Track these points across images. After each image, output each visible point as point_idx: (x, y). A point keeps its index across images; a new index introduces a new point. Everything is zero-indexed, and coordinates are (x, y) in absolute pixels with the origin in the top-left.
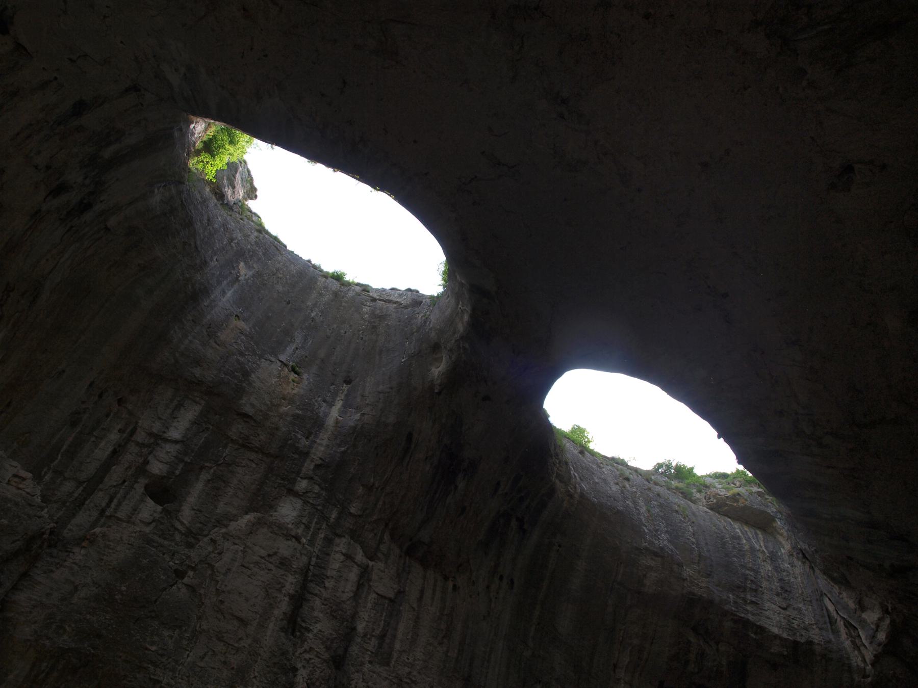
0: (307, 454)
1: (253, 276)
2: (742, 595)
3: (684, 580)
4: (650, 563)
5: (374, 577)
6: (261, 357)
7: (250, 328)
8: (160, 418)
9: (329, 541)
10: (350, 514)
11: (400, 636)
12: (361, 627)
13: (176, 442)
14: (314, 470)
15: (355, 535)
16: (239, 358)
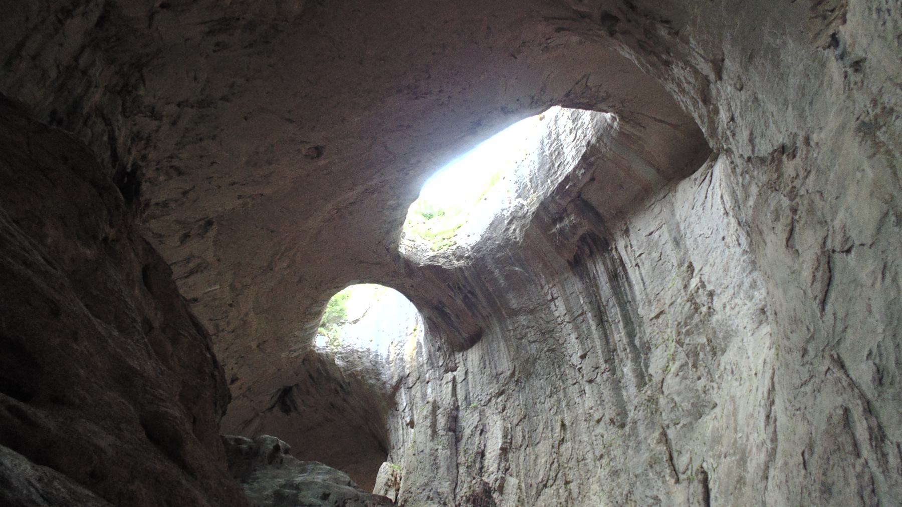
2: (553, 171)
3: (527, 212)
4: (513, 227)
5: (457, 377)
9: (440, 385)
10: (441, 366)
11: (470, 389)
12: (460, 404)
15: (446, 371)
16: (398, 357)
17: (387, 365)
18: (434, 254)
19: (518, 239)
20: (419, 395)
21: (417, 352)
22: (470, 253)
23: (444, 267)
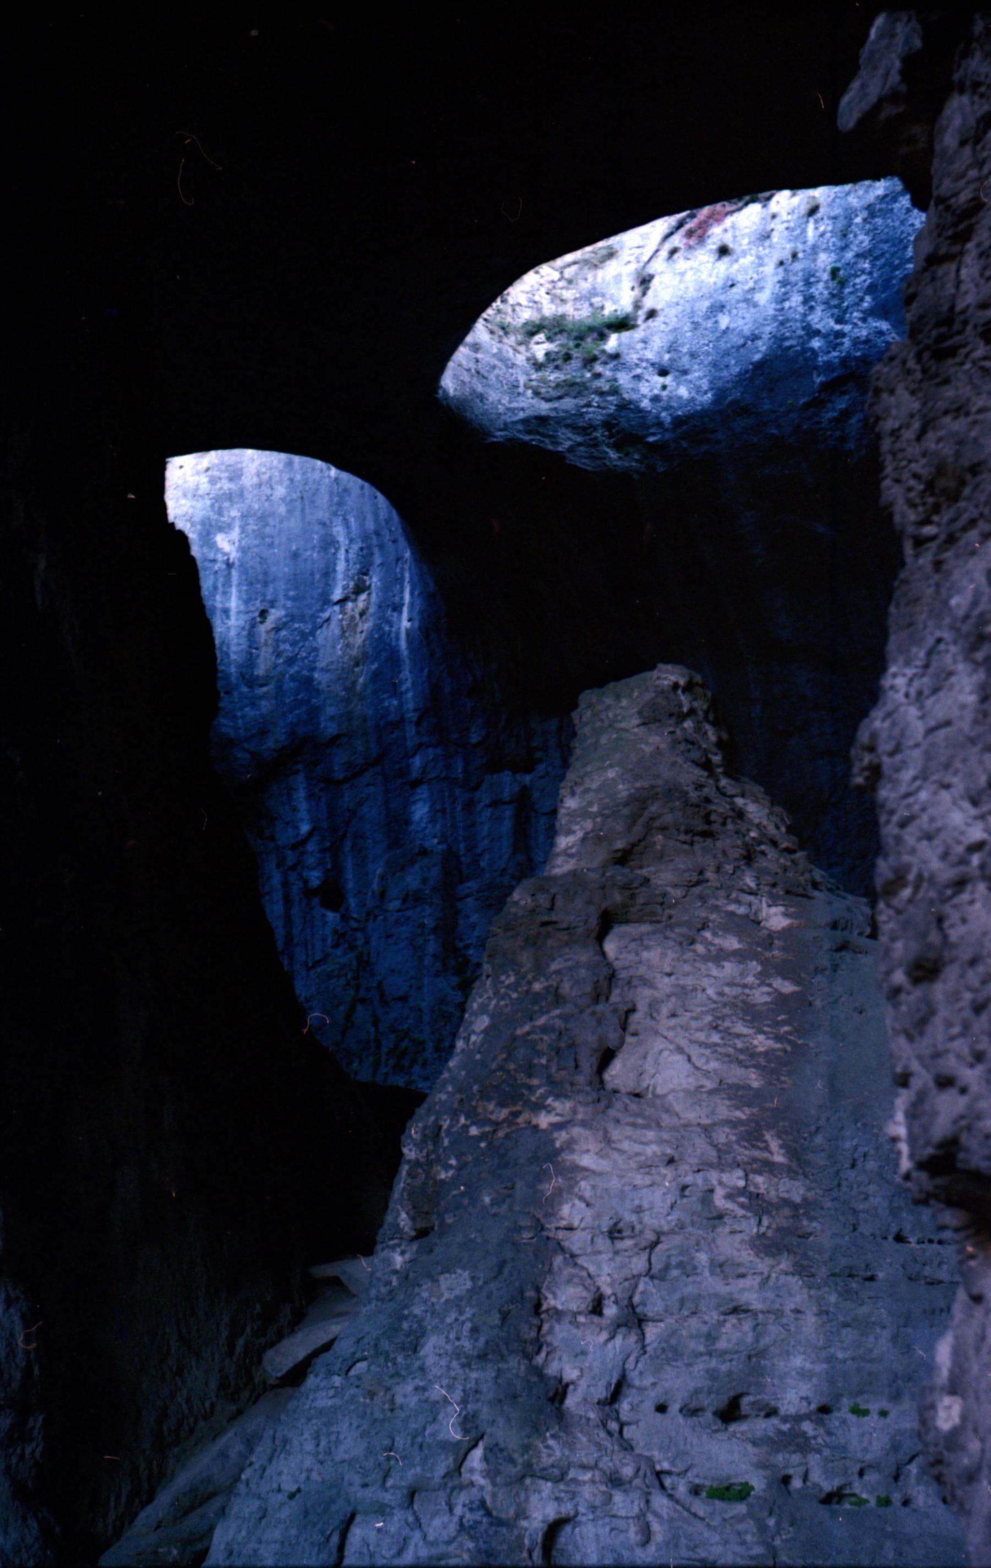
0: (402, 720)
1: (243, 530)
4: (842, 403)
5: (536, 794)
6: (313, 633)
7: (284, 607)
8: (287, 823)
13: (310, 834)
14: (418, 732)
15: (495, 767)
16: (292, 671)
17: (245, 689)
18: (544, 408)
19: (851, 445)
20: (371, 811)
21: (376, 676)
22: (668, 436)
23: (572, 459)
